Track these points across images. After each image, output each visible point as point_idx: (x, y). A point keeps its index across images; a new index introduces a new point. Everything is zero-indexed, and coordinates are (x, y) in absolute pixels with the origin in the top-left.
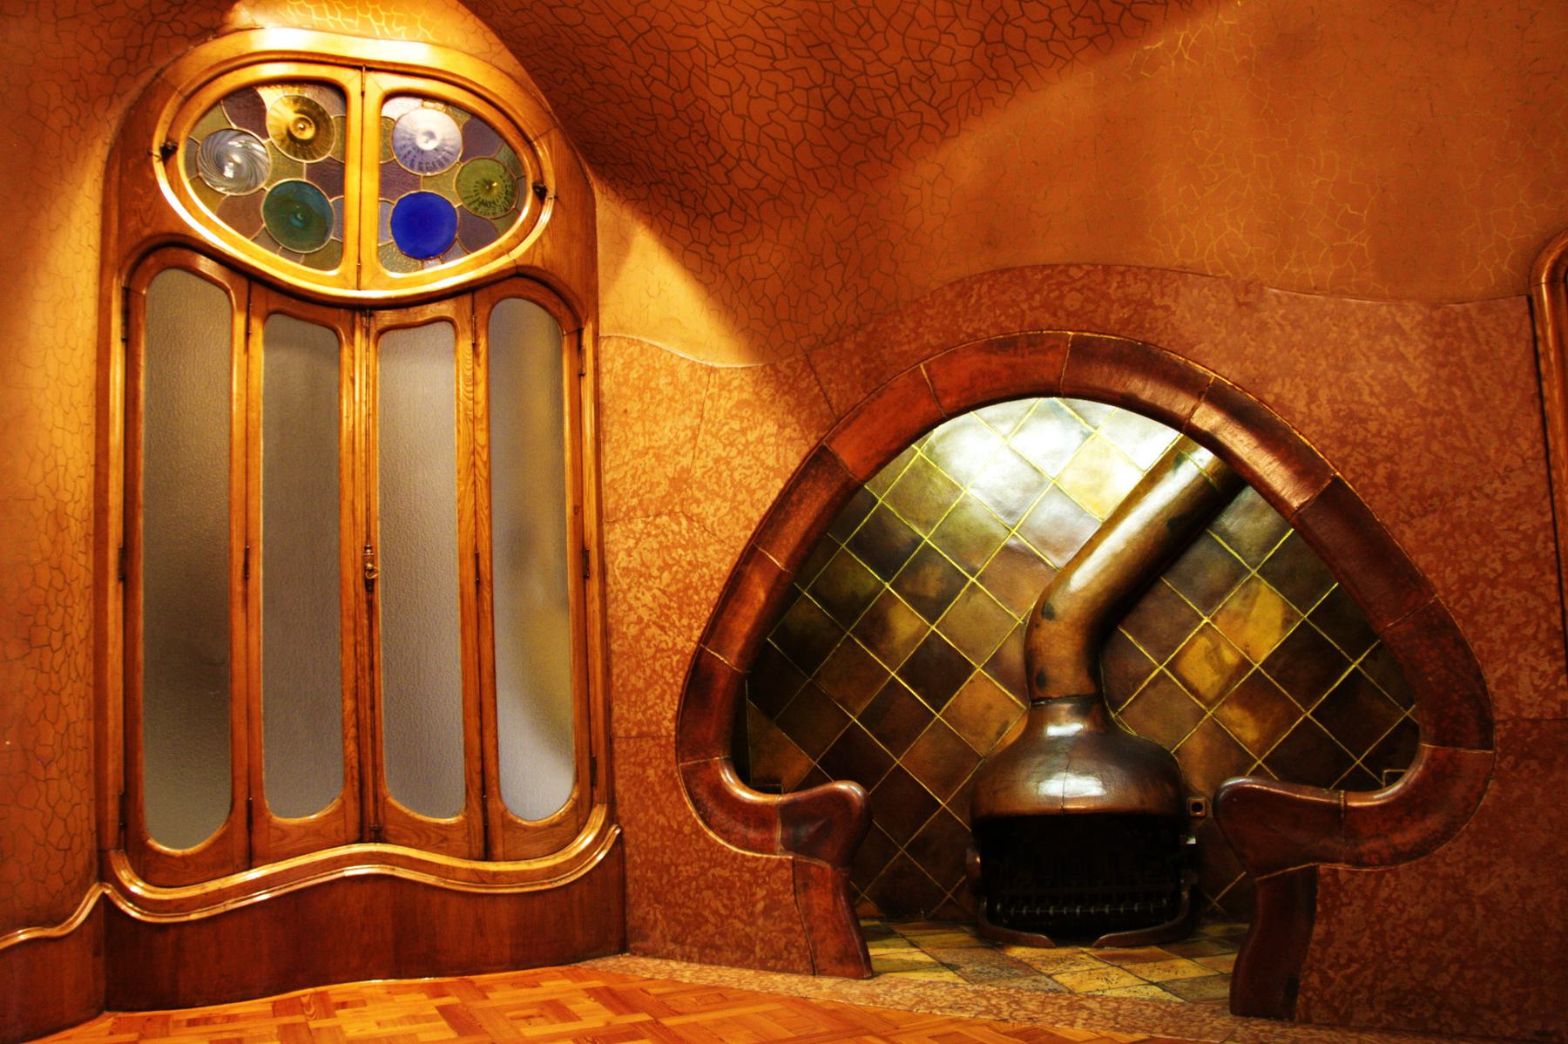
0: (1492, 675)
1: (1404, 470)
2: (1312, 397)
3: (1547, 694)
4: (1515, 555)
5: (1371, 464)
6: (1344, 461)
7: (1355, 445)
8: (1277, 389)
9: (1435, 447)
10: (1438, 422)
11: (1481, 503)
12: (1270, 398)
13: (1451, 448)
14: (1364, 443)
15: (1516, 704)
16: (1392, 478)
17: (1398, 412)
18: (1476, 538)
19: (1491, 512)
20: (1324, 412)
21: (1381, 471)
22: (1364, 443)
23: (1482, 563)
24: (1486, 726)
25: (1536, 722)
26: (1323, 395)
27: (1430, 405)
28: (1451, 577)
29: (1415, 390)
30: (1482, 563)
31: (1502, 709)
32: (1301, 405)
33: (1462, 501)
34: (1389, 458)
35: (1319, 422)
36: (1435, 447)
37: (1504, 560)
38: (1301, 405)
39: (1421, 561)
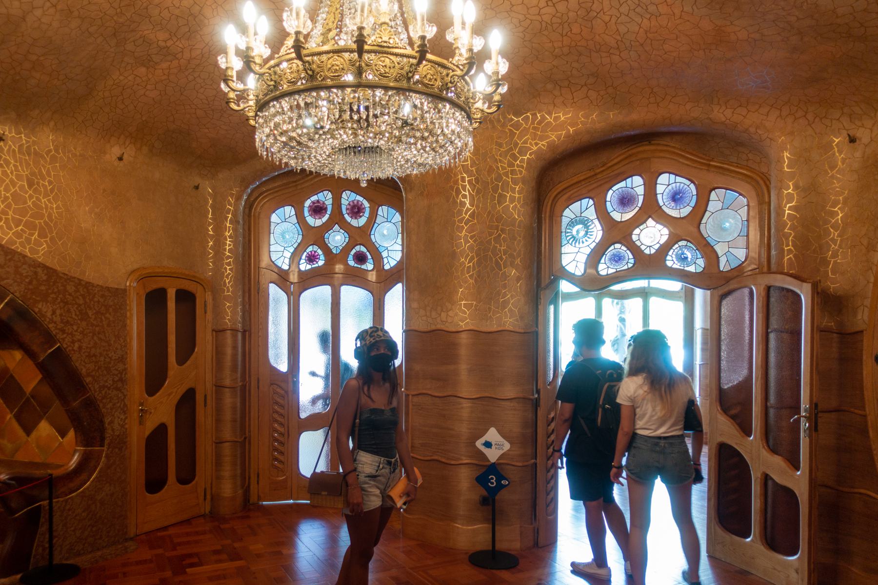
0: (107, 420)
1: (84, 345)
2: (54, 313)
3: (122, 426)
4: (116, 379)
5: (73, 342)
6: (63, 339)
7: (68, 334)
8: (40, 306)
9: (95, 338)
10: (97, 329)
11: (108, 360)
12: (37, 310)
13: (100, 339)
14: (71, 334)
15: (113, 430)
16: (80, 348)
17: (84, 323)
18: (105, 372)
19: (110, 363)
20: (57, 319)
21: (77, 345)
22: (71, 334)
23: (106, 381)
24: (103, 439)
25: (118, 436)
26: (58, 312)
27: (95, 322)
28: (97, 386)
29: (90, 314)
30: (106, 381)
31: (108, 434)
32: (49, 314)
33: (102, 359)
34: (79, 341)
35: (55, 323)
36: (95, 338)
37: (113, 380)
38: (49, 314)
39: (88, 380)
